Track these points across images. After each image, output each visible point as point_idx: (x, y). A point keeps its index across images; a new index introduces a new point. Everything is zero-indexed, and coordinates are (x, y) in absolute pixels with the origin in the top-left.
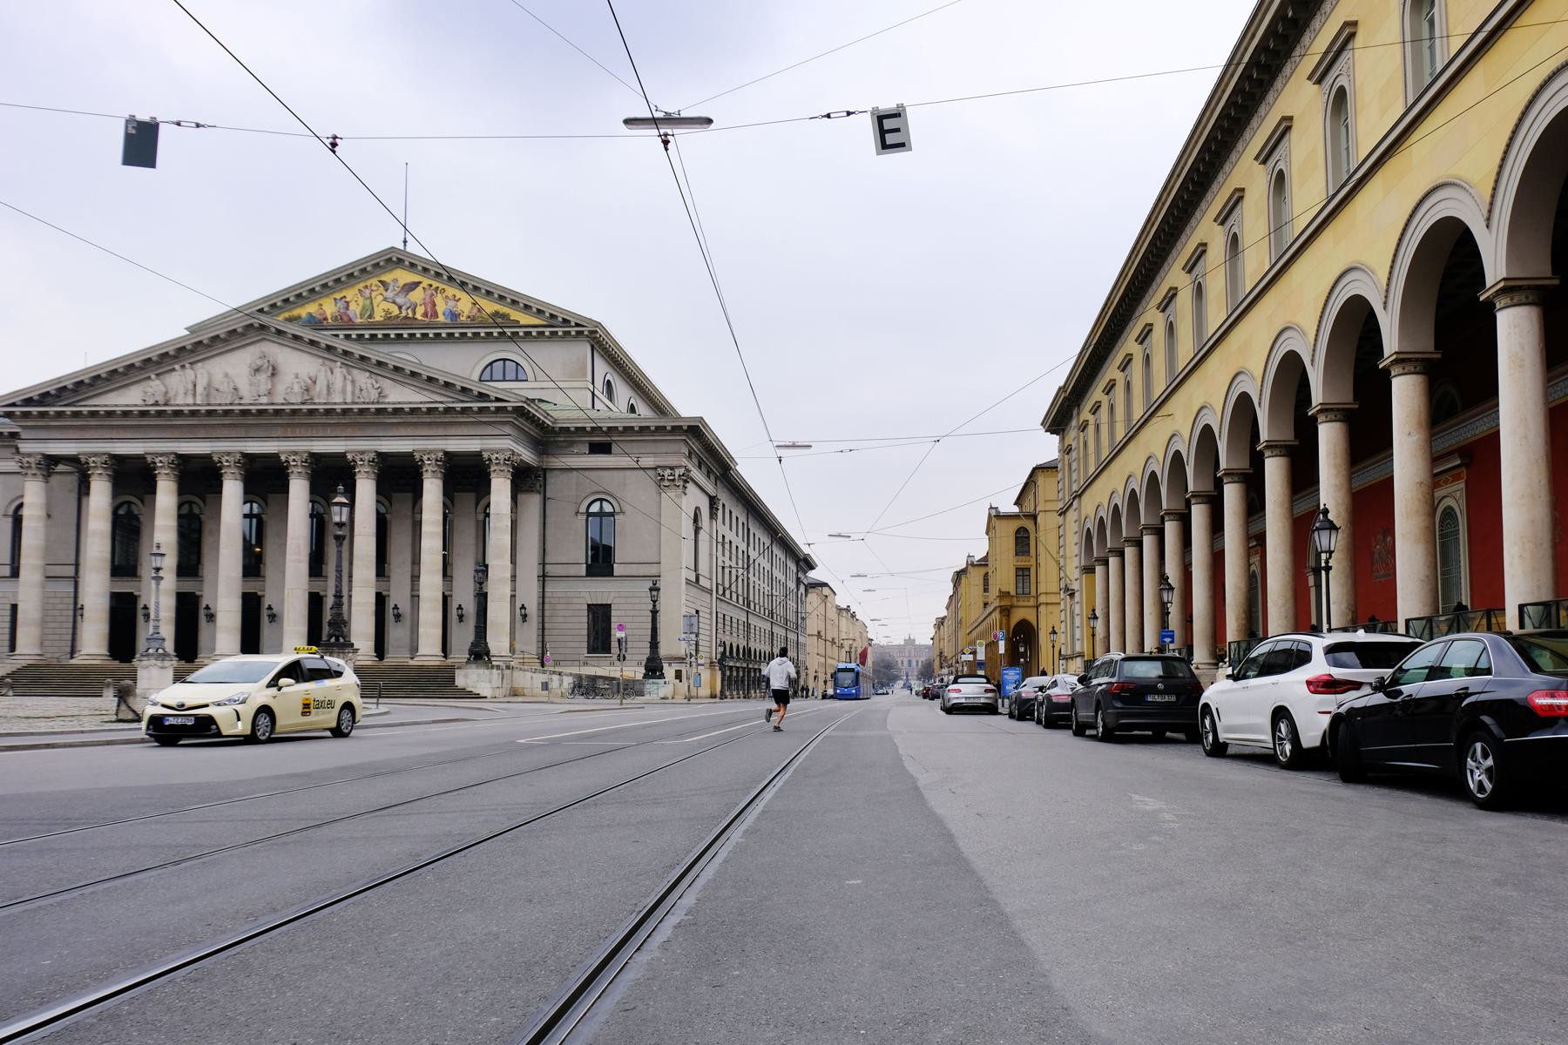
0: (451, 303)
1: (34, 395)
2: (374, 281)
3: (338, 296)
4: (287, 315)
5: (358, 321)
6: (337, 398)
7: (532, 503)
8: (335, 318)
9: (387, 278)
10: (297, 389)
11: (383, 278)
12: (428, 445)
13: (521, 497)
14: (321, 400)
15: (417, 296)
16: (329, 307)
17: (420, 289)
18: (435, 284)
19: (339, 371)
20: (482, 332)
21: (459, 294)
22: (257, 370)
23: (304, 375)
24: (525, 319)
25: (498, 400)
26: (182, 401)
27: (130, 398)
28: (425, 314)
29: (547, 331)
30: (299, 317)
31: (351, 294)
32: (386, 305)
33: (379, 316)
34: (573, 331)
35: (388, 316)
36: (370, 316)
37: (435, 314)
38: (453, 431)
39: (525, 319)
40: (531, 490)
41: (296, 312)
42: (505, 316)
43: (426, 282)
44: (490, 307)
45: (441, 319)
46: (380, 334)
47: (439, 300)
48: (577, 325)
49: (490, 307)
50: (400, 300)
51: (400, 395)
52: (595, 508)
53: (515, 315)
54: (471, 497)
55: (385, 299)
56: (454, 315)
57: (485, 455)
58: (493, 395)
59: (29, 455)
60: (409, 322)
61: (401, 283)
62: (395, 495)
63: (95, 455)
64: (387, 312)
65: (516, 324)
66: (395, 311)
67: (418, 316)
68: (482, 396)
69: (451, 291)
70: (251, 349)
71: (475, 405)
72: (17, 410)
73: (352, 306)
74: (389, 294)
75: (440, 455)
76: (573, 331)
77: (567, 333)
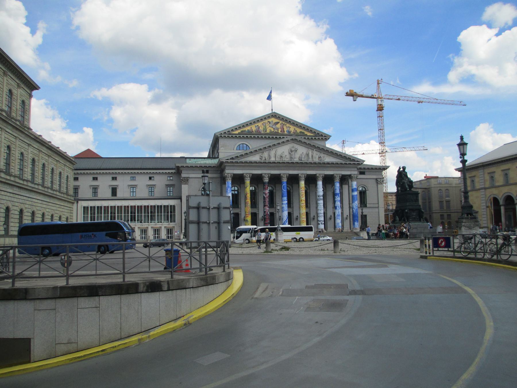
0: (288, 129)
2: (266, 121)
3: (256, 125)
4: (242, 130)
6: (314, 160)
7: (345, 187)
8: (256, 131)
9: (270, 120)
10: (303, 156)
11: (269, 120)
12: (338, 173)
13: (344, 186)
14: (310, 160)
15: (279, 126)
16: (254, 128)
19: (315, 152)
21: (290, 126)
22: (292, 151)
23: (305, 153)
24: (309, 134)
26: (273, 159)
27: (256, 158)
28: (281, 131)
29: (317, 138)
30: (245, 131)
31: (260, 124)
33: (268, 131)
34: (324, 138)
36: (266, 131)
39: (309, 134)
40: (346, 184)
42: (303, 133)
43: (281, 122)
44: (299, 130)
45: (286, 133)
46: (267, 136)
47: (285, 127)
49: (299, 130)
51: (328, 159)
52: (361, 189)
53: (306, 133)
54: (331, 185)
56: (289, 132)
58: (356, 160)
59: (228, 174)
60: (277, 134)
61: (274, 122)
62: (311, 185)
63: (247, 174)
64: (270, 130)
66: (273, 130)
67: (279, 132)
68: (354, 160)
69: (288, 125)
71: (352, 163)
73: (260, 128)
74: (271, 125)
76: (324, 138)
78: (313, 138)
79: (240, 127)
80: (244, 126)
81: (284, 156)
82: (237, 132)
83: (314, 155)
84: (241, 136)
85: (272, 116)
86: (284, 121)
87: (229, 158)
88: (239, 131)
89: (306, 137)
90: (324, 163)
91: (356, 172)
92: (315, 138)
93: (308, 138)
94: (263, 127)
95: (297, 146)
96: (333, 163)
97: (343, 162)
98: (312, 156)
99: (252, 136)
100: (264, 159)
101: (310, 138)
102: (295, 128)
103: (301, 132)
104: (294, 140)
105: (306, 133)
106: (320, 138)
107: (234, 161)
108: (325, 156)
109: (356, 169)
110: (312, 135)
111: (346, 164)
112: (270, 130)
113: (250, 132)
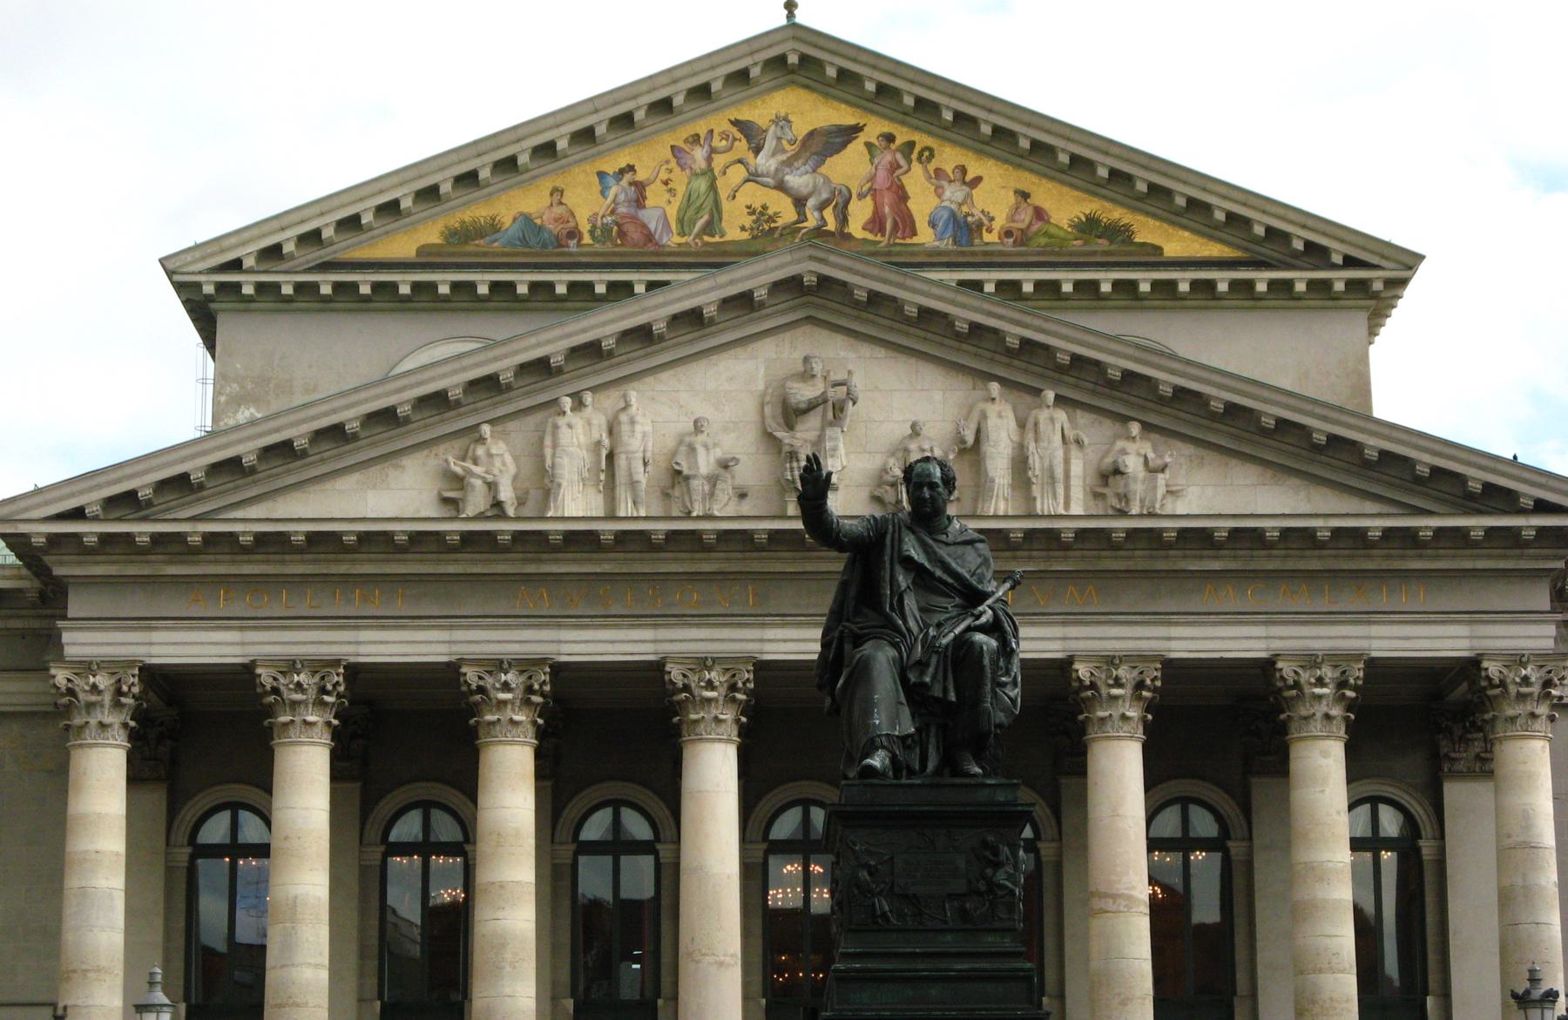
0: (954, 193)
1: (143, 484)
2: (718, 122)
4: (454, 221)
5: (673, 240)
6: (1044, 505)
8: (602, 232)
9: (760, 112)
11: (745, 114)
12: (1320, 639)
15: (850, 167)
17: (856, 148)
18: (902, 135)
20: (1067, 280)
22: (792, 414)
25: (1542, 507)
28: (876, 223)
29: (1262, 279)
30: (493, 227)
31: (648, 157)
32: (754, 195)
33: (734, 228)
34: (1339, 279)
35: (766, 234)
37: (906, 224)
38: (1382, 601)
39: (1178, 244)
41: (476, 211)
42: (1117, 232)
43: (875, 128)
45: (926, 236)
47: (916, 181)
48: (1350, 262)
49: (1066, 207)
50: (798, 180)
53: (1148, 231)
55: (753, 177)
56: (964, 228)
57: (1493, 668)
58: (1529, 493)
61: (801, 128)
64: (761, 215)
65: (1152, 258)
67: (856, 228)
68: (1497, 497)
69: (949, 157)
70: (767, 349)
71: (1477, 523)
72: (88, 530)
73: (655, 196)
74: (765, 162)
75: (1357, 672)
76: (1339, 279)
77: (1320, 288)
78: (1222, 280)
79: (430, 194)
80: (468, 179)
81: (705, 463)
82: (402, 246)
83: (1049, 450)
84: (443, 281)
85: (781, 60)
86: (904, 116)
87: (91, 499)
88: (432, 234)
89: (1145, 280)
90: (1153, 536)
91: (1540, 636)
92: (1243, 288)
93: (1166, 289)
94: (680, 182)
95: (841, 357)
96: (1247, 538)
97: (1376, 523)
98: (1020, 464)
99: (561, 281)
100: (477, 501)
101: (1183, 280)
102: (1027, 181)
103: (1089, 226)
104: (817, 299)
105: (1148, 231)
106: (1300, 279)
107: (142, 530)
108: (1175, 454)
109: (1541, 598)
110: (1215, 250)
111: (1408, 538)
112: (761, 215)
113: (544, 245)
